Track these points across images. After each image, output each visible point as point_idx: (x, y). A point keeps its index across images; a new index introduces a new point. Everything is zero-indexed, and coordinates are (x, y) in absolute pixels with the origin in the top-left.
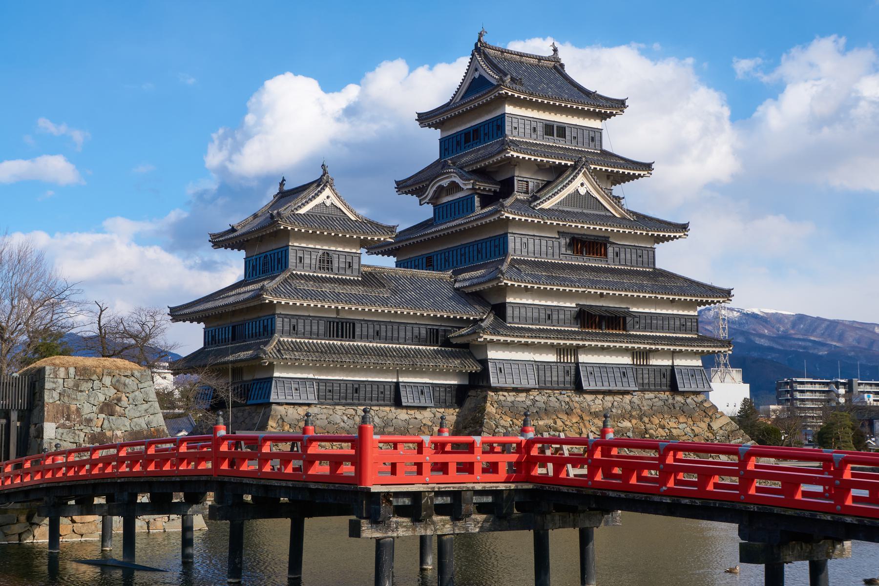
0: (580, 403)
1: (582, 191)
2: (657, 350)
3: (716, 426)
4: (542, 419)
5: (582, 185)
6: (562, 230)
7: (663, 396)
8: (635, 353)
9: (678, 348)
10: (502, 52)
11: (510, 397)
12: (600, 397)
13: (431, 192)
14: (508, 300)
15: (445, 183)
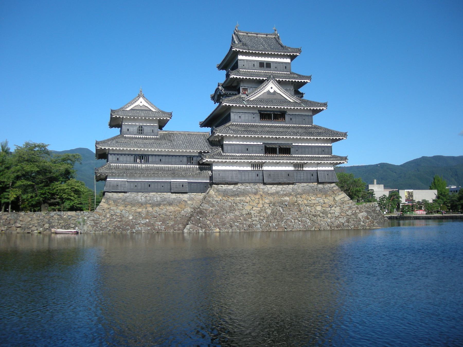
0: (263, 189)
1: (272, 91)
2: (305, 164)
3: (337, 199)
4: (239, 197)
5: (272, 88)
6: (260, 109)
7: (311, 184)
8: (295, 165)
9: (319, 162)
10: (247, 33)
11: (225, 187)
12: (275, 186)
13: (216, 97)
14: (224, 142)
15: (218, 93)
